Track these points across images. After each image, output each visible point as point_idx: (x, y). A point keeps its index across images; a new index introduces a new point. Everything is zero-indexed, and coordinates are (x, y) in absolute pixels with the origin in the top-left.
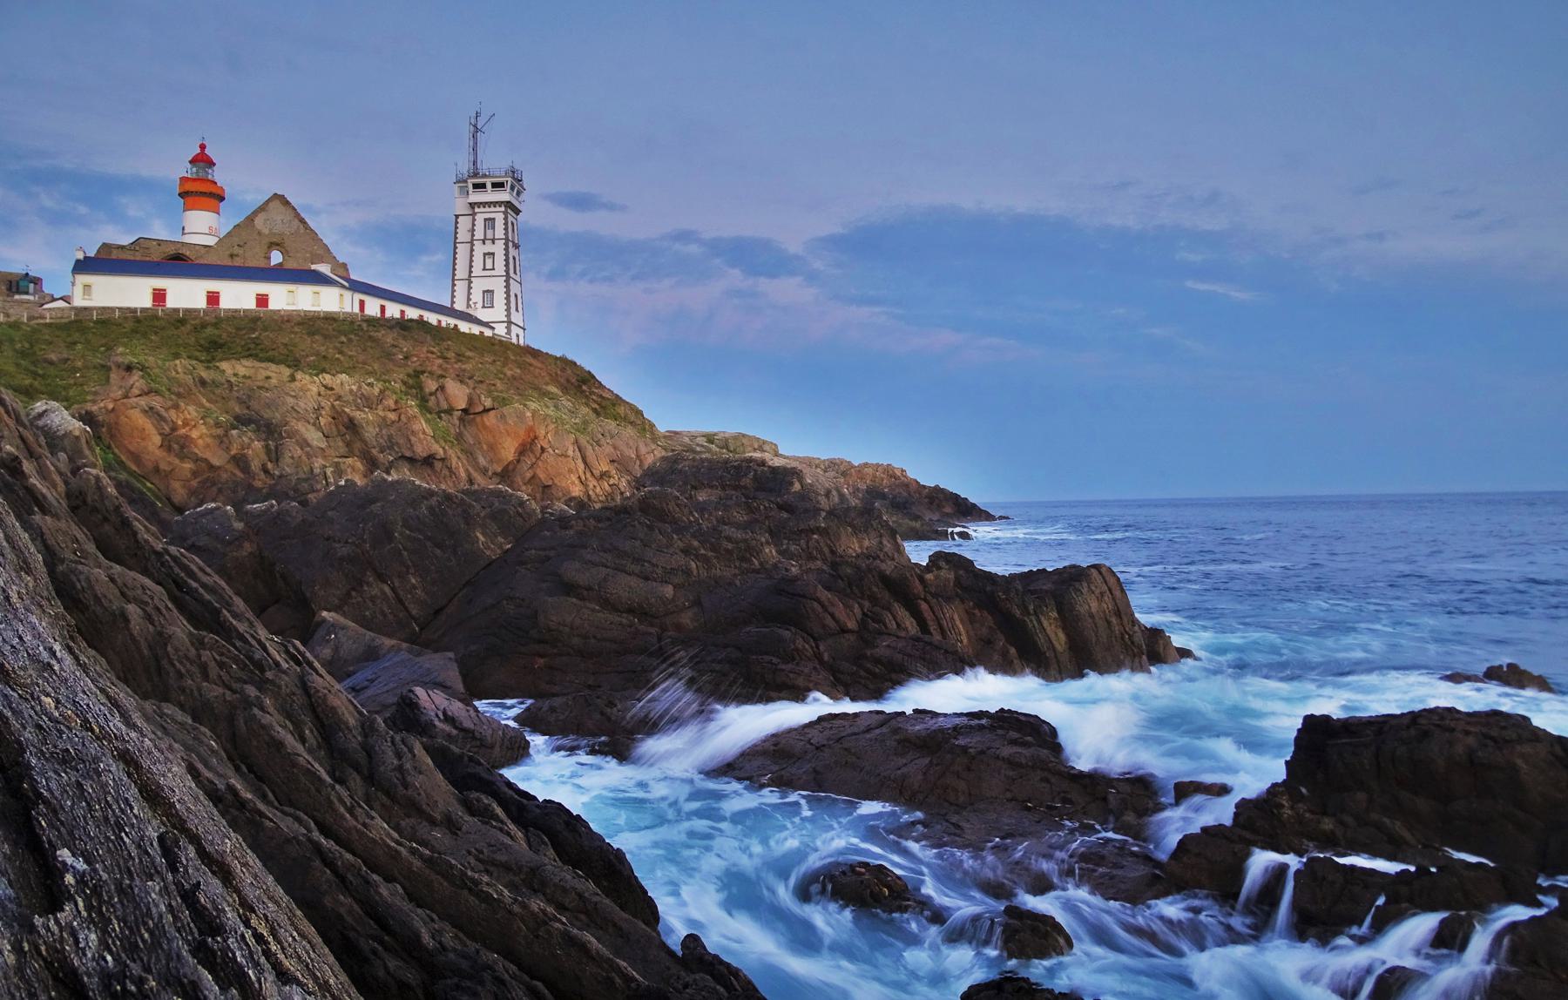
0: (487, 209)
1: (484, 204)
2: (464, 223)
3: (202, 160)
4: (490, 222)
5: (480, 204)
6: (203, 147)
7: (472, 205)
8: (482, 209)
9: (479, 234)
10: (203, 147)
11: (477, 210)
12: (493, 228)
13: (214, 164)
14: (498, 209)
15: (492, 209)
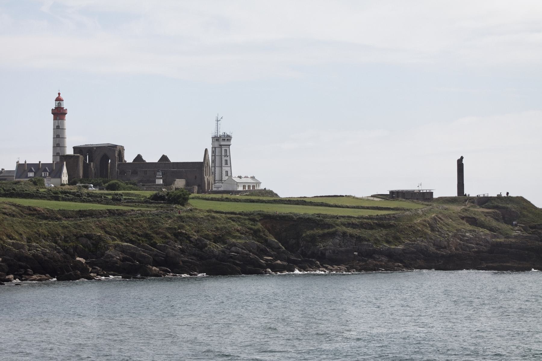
0: (225, 147)
1: (224, 145)
2: (218, 150)
3: (59, 99)
4: (226, 150)
5: (223, 145)
6: (59, 94)
7: (221, 145)
8: (223, 147)
9: (223, 154)
10: (59, 94)
11: (222, 147)
12: (226, 152)
13: (63, 101)
14: (227, 147)
15: (226, 147)
